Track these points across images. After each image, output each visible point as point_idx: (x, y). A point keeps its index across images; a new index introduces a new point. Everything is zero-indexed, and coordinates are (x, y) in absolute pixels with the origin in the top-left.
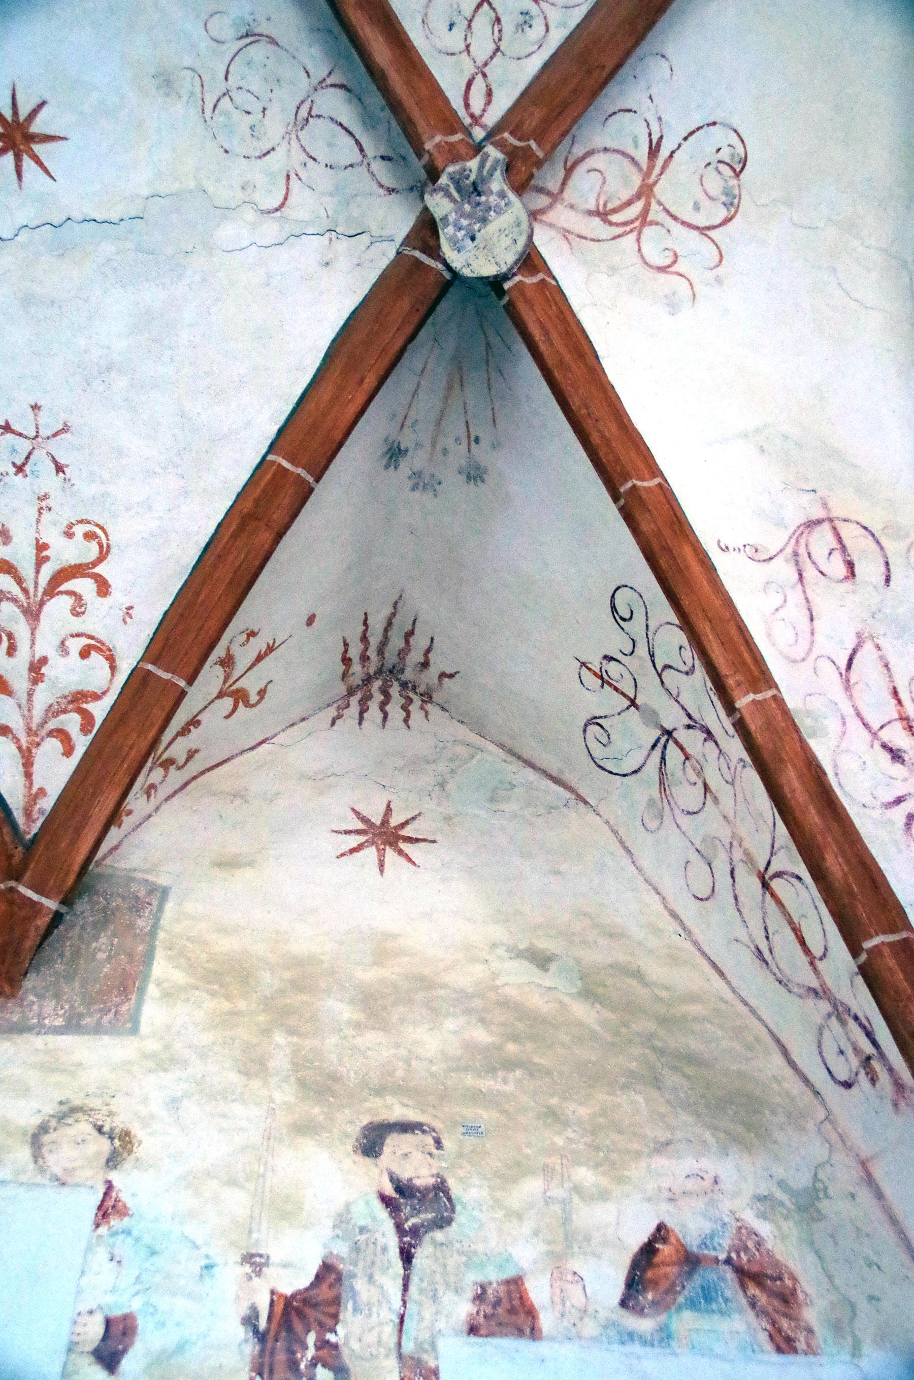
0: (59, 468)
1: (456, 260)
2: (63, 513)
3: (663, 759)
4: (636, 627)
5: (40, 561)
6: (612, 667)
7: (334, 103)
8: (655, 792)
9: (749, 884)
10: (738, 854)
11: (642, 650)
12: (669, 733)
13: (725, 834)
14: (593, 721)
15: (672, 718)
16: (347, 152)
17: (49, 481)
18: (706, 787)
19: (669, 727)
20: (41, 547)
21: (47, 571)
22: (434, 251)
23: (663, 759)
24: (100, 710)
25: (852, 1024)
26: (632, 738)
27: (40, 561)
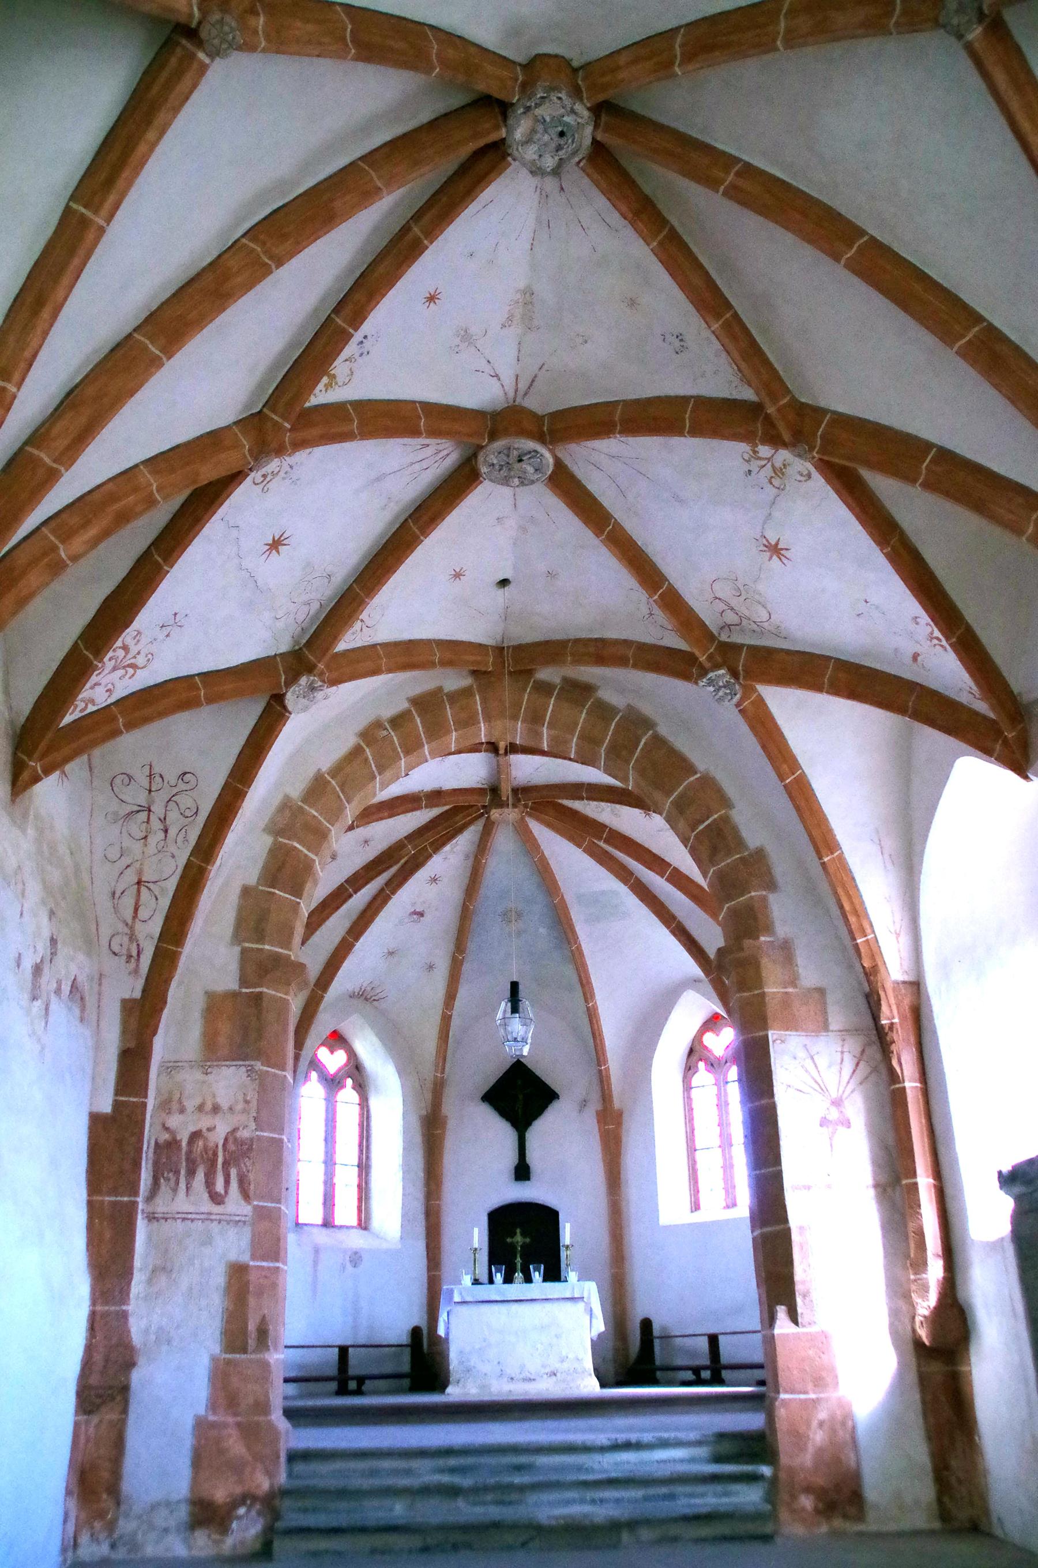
0: (167, 636)
1: (289, 696)
2: (153, 648)
3: (138, 811)
4: (182, 786)
5: (135, 657)
6: (158, 779)
7: (316, 606)
8: (122, 813)
9: (131, 877)
10: (137, 865)
11: (175, 790)
12: (150, 811)
13: (139, 857)
14: (130, 778)
15: (158, 809)
16: (301, 617)
17: (161, 636)
18: (145, 838)
19: (152, 808)
20: (139, 653)
21: (133, 661)
22: (289, 684)
23: (138, 811)
24: (91, 708)
25: (135, 944)
26: (136, 796)
27: (135, 657)
